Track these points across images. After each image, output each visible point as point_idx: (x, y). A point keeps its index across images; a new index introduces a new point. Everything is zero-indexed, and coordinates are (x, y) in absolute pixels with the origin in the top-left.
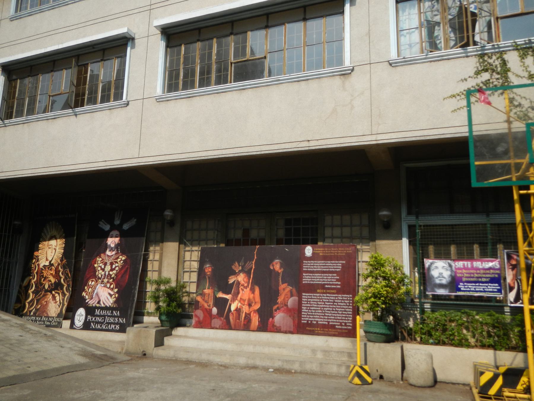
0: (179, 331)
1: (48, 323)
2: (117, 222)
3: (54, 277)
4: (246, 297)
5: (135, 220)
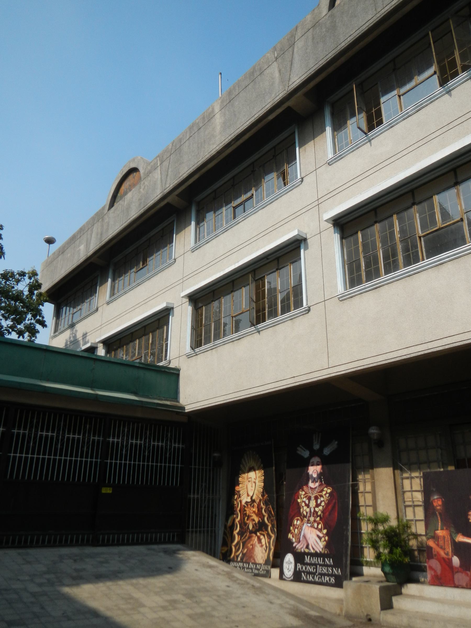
1: (256, 572)
2: (316, 447)
3: (257, 515)
5: (336, 443)
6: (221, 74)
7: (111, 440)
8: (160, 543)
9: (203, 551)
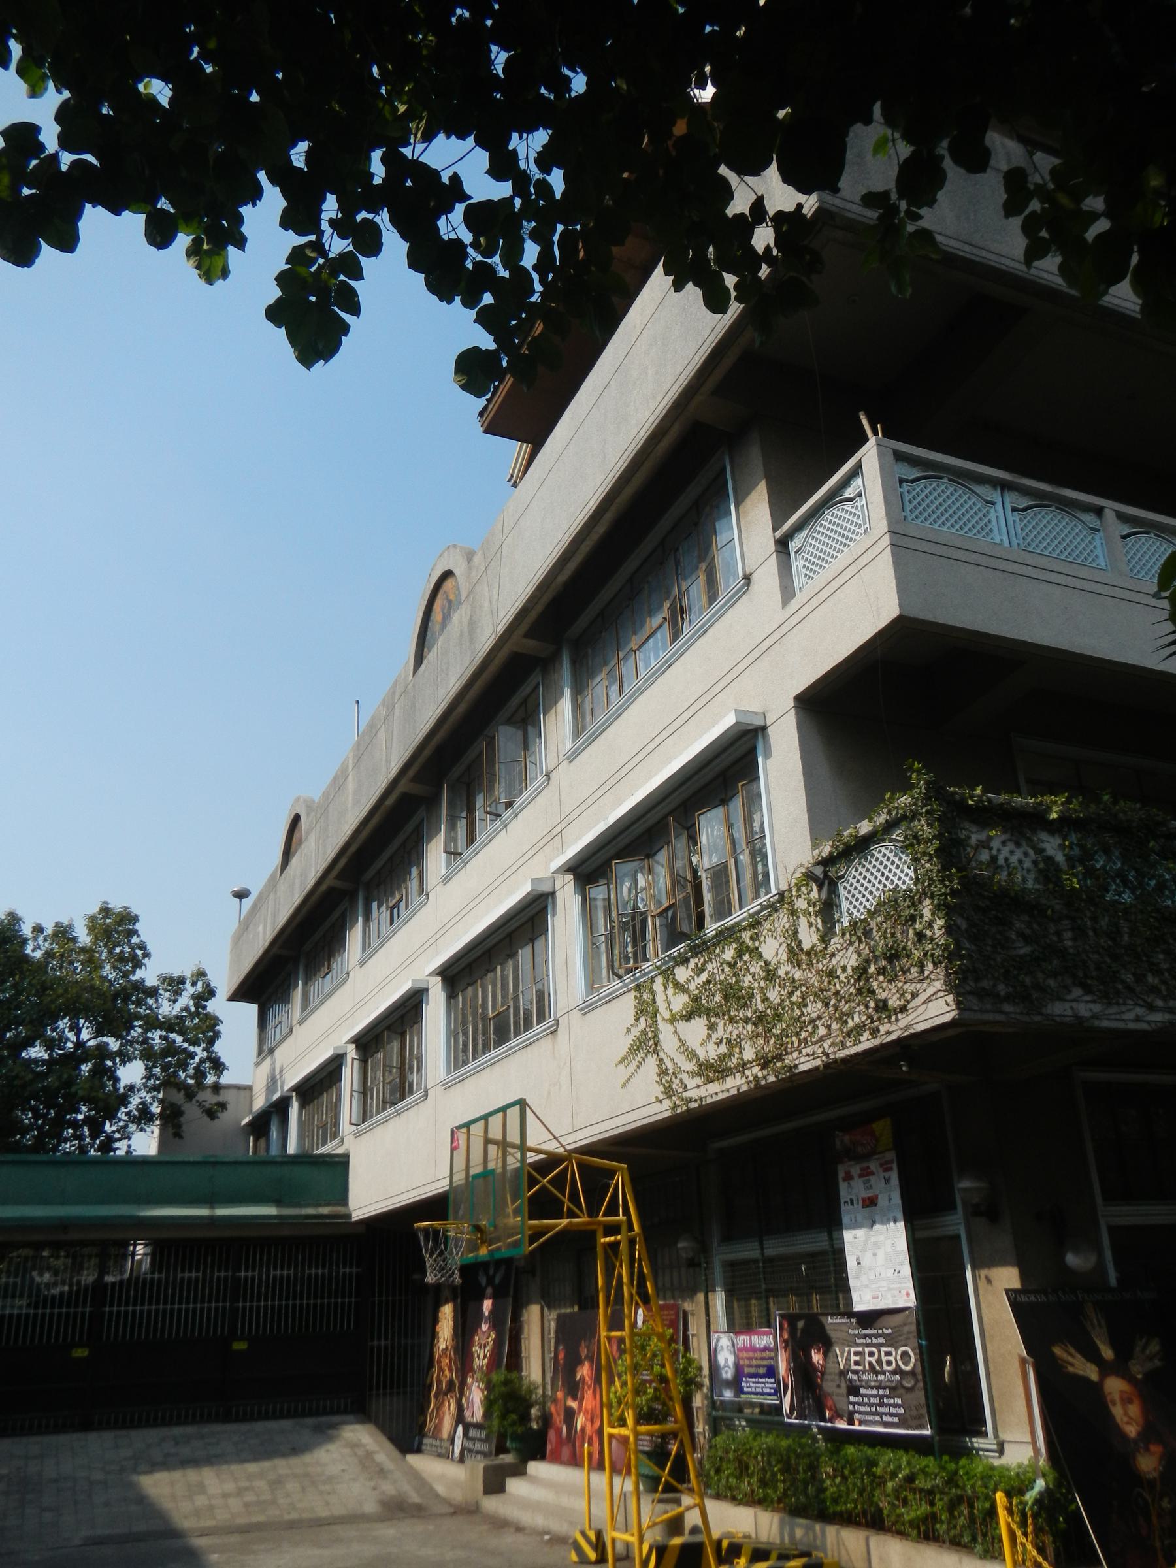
0: (534, 1467)
1: (439, 1451)
2: (491, 1272)
4: (589, 1407)
6: (358, 702)
7: (243, 1274)
8: (311, 1414)
9: (376, 1424)
